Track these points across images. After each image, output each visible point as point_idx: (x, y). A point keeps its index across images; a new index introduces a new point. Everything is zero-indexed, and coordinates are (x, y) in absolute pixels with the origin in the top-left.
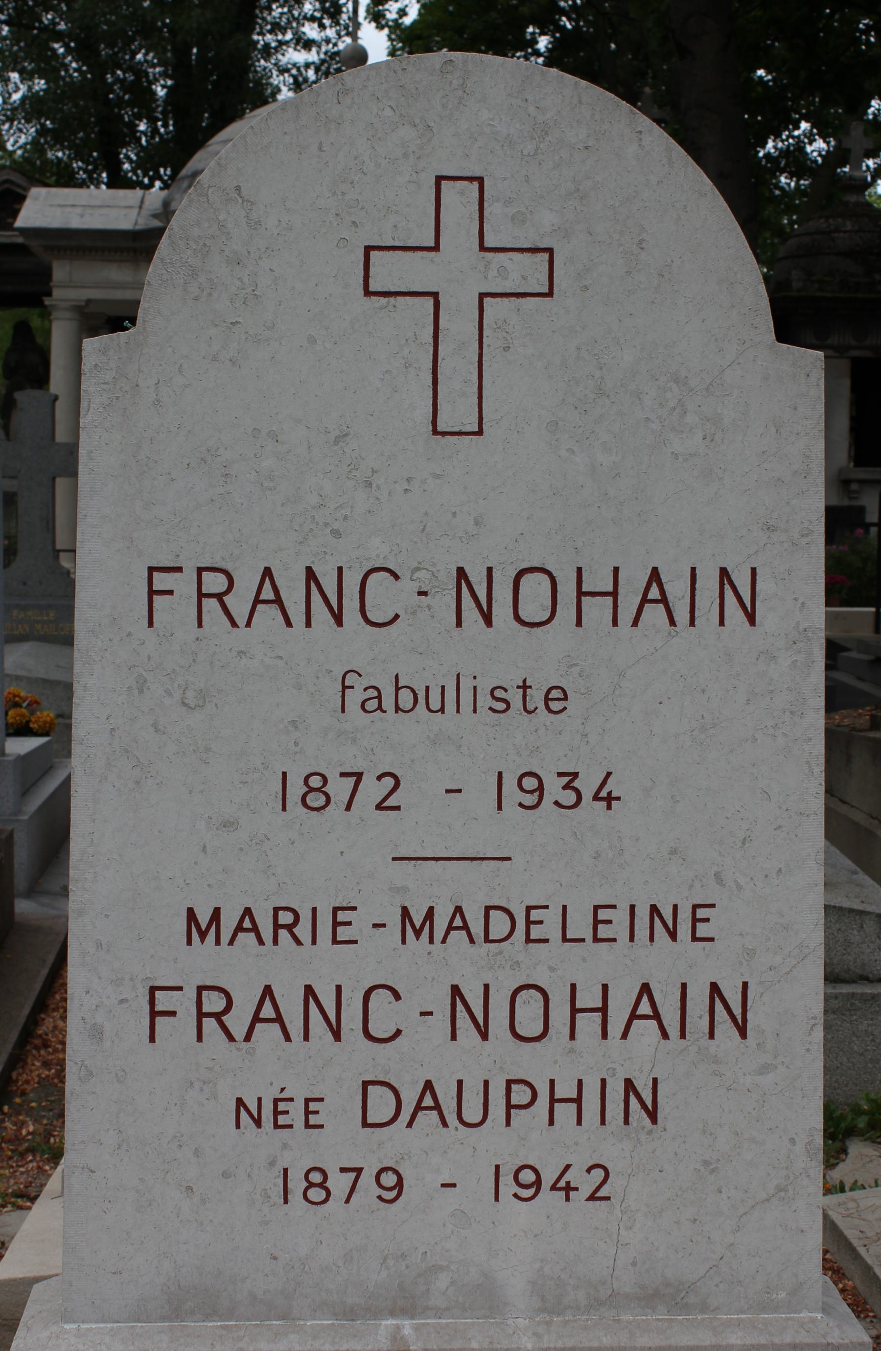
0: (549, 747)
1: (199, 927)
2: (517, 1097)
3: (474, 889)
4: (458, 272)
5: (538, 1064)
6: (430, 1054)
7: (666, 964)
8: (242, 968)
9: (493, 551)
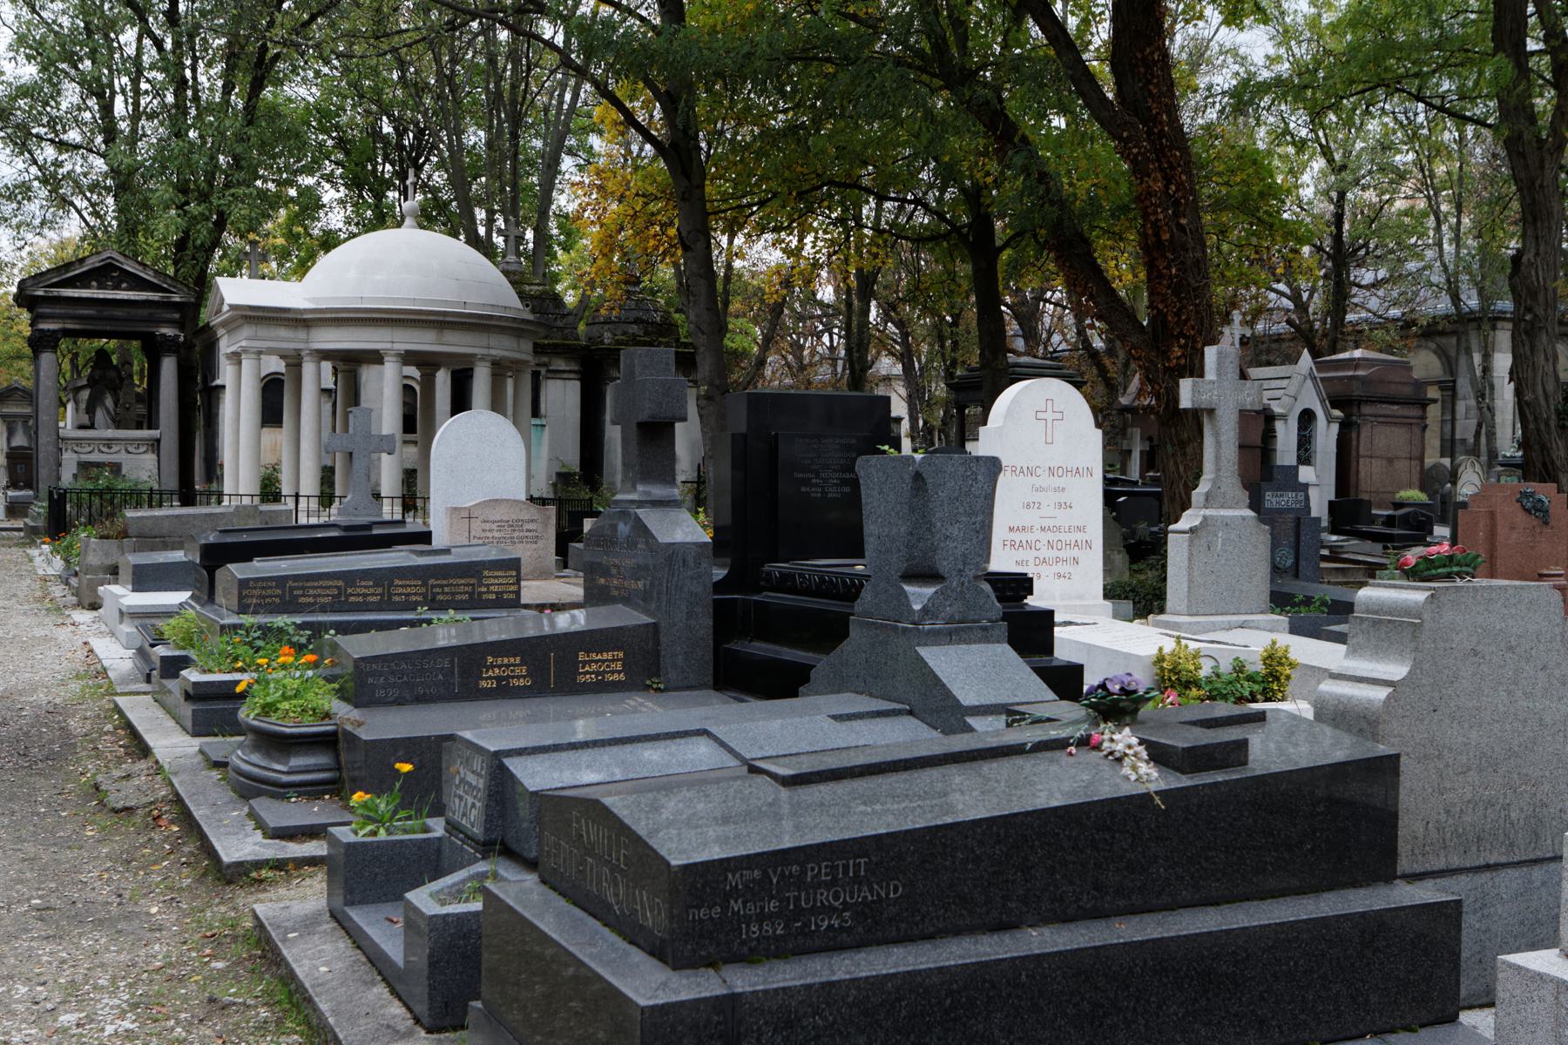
0: (1062, 498)
1: (1011, 529)
2: (1058, 560)
3: (1050, 523)
4: (1049, 416)
5: (1062, 554)
6: (1045, 553)
7: (1079, 536)
8: (1017, 537)
9: (1054, 464)
